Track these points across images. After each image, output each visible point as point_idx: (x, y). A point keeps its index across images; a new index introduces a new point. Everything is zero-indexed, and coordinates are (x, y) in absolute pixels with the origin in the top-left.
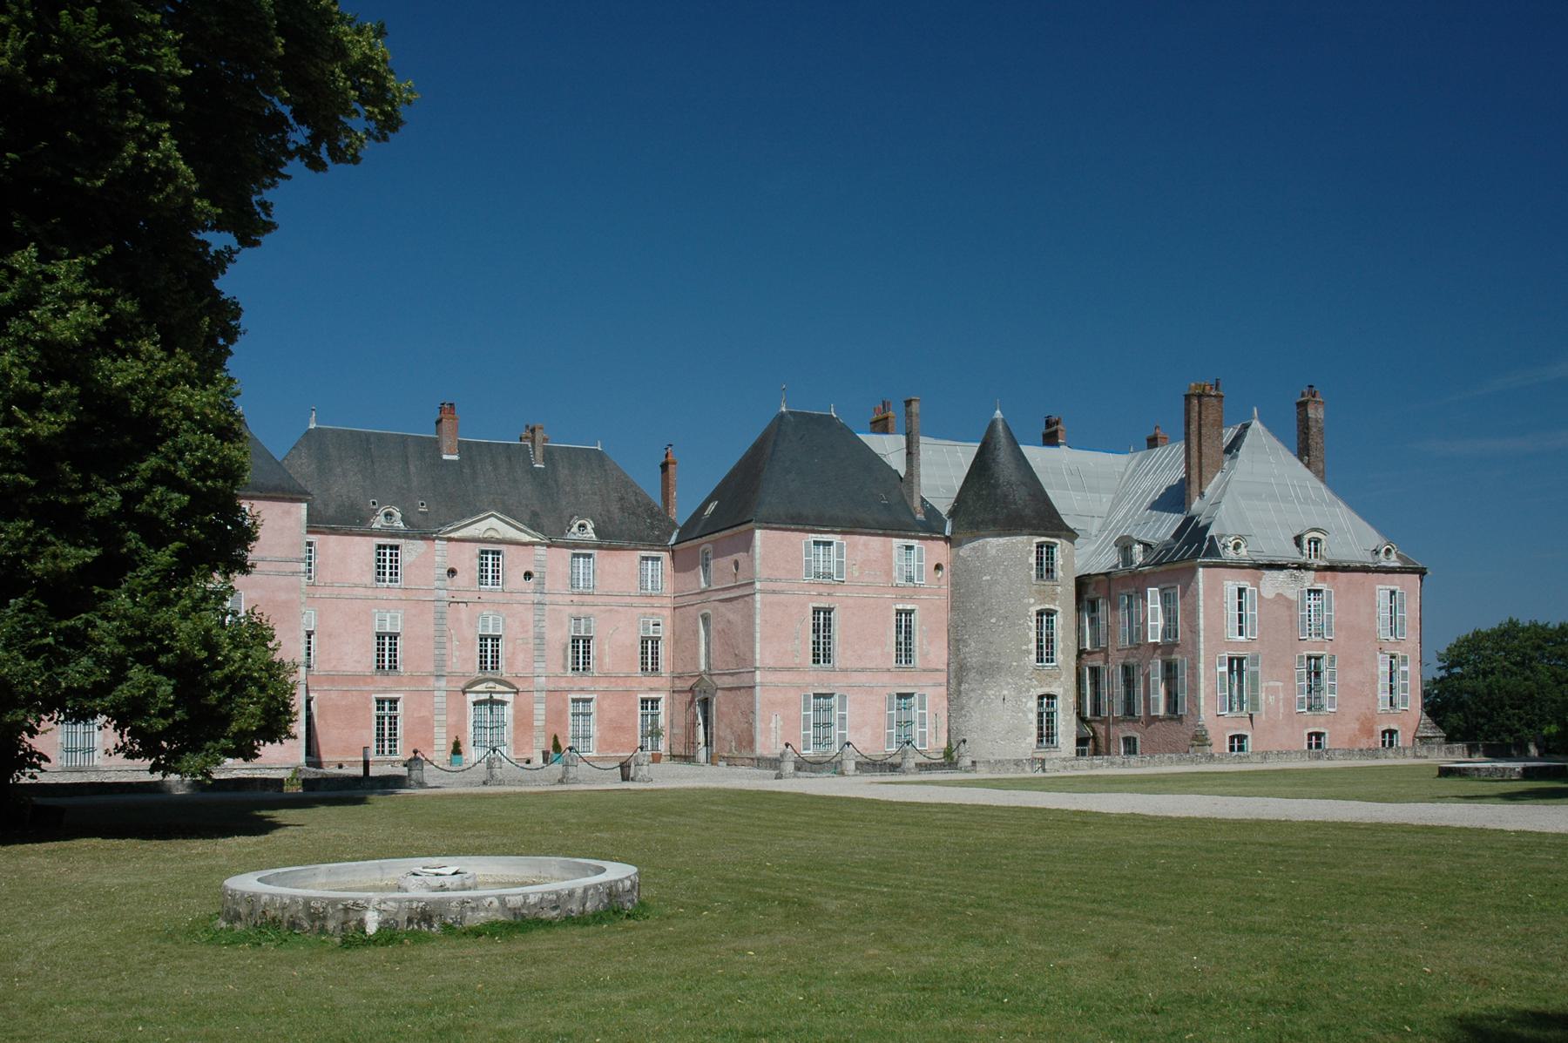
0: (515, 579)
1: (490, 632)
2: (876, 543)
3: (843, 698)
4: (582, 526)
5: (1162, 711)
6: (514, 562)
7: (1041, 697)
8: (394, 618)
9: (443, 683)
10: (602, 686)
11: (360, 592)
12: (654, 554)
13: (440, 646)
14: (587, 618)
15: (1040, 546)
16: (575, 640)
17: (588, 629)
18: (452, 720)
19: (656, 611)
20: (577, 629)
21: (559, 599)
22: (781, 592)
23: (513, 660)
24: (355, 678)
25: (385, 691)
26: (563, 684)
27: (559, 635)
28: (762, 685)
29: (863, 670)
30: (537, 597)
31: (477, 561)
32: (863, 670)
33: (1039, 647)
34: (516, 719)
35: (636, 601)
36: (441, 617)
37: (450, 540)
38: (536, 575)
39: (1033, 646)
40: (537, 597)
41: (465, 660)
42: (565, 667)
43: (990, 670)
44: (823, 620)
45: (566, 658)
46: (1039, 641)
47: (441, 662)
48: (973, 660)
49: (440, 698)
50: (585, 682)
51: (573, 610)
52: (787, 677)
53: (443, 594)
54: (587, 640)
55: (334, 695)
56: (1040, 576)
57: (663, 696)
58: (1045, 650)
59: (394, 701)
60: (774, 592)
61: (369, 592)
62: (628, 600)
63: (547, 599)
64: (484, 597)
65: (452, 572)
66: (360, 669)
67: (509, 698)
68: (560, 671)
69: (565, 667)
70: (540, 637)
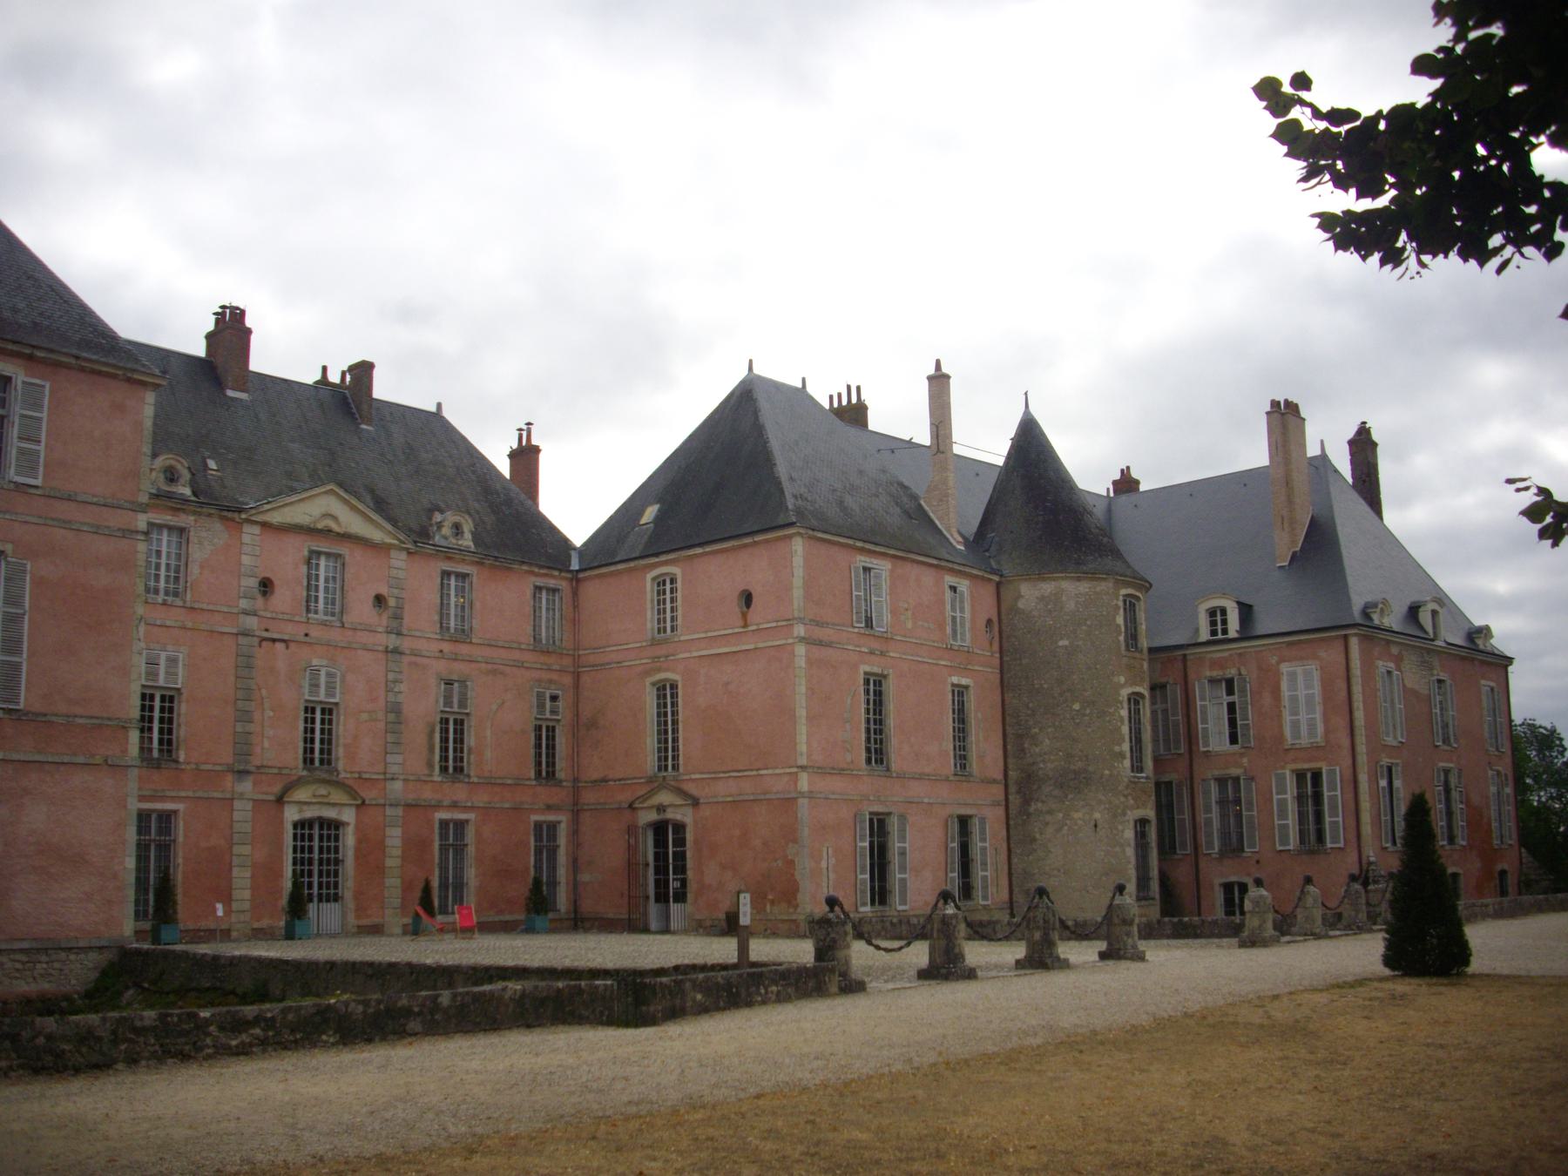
0: (361, 609)
1: (322, 697)
3: (903, 818)
4: (457, 527)
5: (1293, 842)
8: (172, 661)
9: (246, 786)
10: (481, 799)
12: (552, 583)
13: (245, 717)
14: (463, 683)
17: (463, 704)
19: (554, 676)
20: (448, 702)
21: (421, 645)
22: (829, 645)
23: (357, 742)
26: (427, 794)
27: (423, 706)
28: (811, 795)
29: (920, 777)
30: (393, 641)
31: (304, 569)
32: (920, 777)
35: (529, 658)
36: (245, 664)
37: (265, 525)
38: (392, 602)
40: (393, 641)
41: (279, 743)
43: (1075, 781)
45: (431, 749)
47: (243, 747)
50: (460, 792)
51: (440, 666)
53: (251, 623)
54: (459, 723)
57: (563, 819)
59: (166, 818)
60: (820, 643)
62: (517, 655)
63: (406, 644)
64: (316, 633)
65: (266, 586)
67: (348, 816)
69: (430, 765)
70: (395, 709)
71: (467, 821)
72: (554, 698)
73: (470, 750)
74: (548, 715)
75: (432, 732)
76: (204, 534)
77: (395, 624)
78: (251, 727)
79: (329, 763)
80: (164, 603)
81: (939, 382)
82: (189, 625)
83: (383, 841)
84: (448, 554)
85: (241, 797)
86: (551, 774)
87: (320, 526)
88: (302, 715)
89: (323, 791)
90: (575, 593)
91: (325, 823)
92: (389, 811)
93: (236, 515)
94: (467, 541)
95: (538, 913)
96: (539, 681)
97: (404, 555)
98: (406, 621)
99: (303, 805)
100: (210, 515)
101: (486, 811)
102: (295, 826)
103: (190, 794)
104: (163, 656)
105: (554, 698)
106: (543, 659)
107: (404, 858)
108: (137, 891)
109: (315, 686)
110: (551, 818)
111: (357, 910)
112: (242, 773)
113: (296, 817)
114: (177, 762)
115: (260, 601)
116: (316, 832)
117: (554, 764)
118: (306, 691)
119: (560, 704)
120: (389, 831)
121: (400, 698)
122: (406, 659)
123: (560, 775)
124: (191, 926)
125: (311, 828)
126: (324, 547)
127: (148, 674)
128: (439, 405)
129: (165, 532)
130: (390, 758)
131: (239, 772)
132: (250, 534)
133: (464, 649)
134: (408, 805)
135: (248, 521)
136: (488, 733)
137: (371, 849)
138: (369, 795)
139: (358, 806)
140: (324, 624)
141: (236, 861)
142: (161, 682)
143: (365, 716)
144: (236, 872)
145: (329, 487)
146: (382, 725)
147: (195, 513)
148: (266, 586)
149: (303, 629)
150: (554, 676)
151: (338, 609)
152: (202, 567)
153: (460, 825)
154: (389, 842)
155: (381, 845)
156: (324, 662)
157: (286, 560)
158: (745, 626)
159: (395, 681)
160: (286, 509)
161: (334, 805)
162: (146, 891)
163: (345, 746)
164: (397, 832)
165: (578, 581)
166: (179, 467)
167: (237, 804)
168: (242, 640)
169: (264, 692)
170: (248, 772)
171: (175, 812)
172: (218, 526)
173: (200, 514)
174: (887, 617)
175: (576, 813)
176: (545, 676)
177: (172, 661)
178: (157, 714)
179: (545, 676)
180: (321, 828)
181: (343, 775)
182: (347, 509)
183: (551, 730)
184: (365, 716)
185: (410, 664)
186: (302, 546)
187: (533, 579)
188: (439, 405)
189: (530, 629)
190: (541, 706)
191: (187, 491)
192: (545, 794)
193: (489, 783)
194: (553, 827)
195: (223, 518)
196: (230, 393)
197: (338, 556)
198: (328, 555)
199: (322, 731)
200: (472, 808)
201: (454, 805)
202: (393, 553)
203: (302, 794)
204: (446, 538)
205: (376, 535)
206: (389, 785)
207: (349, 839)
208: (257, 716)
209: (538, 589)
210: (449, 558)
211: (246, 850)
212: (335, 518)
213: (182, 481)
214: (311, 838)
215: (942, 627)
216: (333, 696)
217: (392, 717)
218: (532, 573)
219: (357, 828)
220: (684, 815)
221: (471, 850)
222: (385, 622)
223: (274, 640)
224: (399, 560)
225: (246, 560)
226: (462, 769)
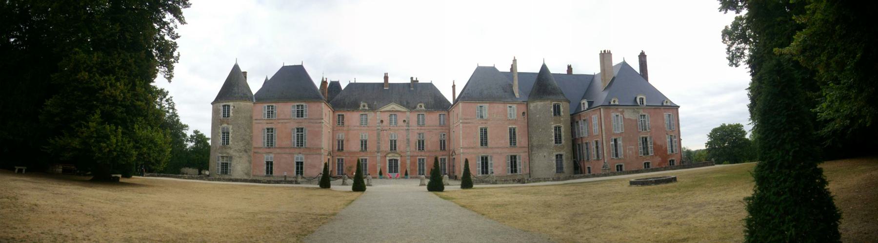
0: (400, 123)
2: (501, 106)
6: (401, 118)
7: (557, 156)
10: (427, 154)
15: (554, 106)
23: (400, 146)
24: (354, 153)
27: (414, 138)
33: (556, 139)
36: (378, 135)
39: (554, 138)
41: (386, 146)
43: (540, 147)
44: (484, 133)
46: (556, 136)
47: (379, 148)
48: (535, 144)
49: (379, 158)
50: (423, 153)
52: (471, 150)
56: (555, 115)
57: (447, 158)
58: (558, 139)
65: (382, 121)
67: (399, 158)
70: (408, 140)
81: (515, 61)
84: (418, 111)
94: (423, 108)
99: (391, 156)
132: (378, 113)
148: (382, 121)
151: (396, 123)
174: (487, 115)
186: (389, 114)
193: (429, 151)
207: (399, 162)
215: (506, 116)
224: (408, 113)
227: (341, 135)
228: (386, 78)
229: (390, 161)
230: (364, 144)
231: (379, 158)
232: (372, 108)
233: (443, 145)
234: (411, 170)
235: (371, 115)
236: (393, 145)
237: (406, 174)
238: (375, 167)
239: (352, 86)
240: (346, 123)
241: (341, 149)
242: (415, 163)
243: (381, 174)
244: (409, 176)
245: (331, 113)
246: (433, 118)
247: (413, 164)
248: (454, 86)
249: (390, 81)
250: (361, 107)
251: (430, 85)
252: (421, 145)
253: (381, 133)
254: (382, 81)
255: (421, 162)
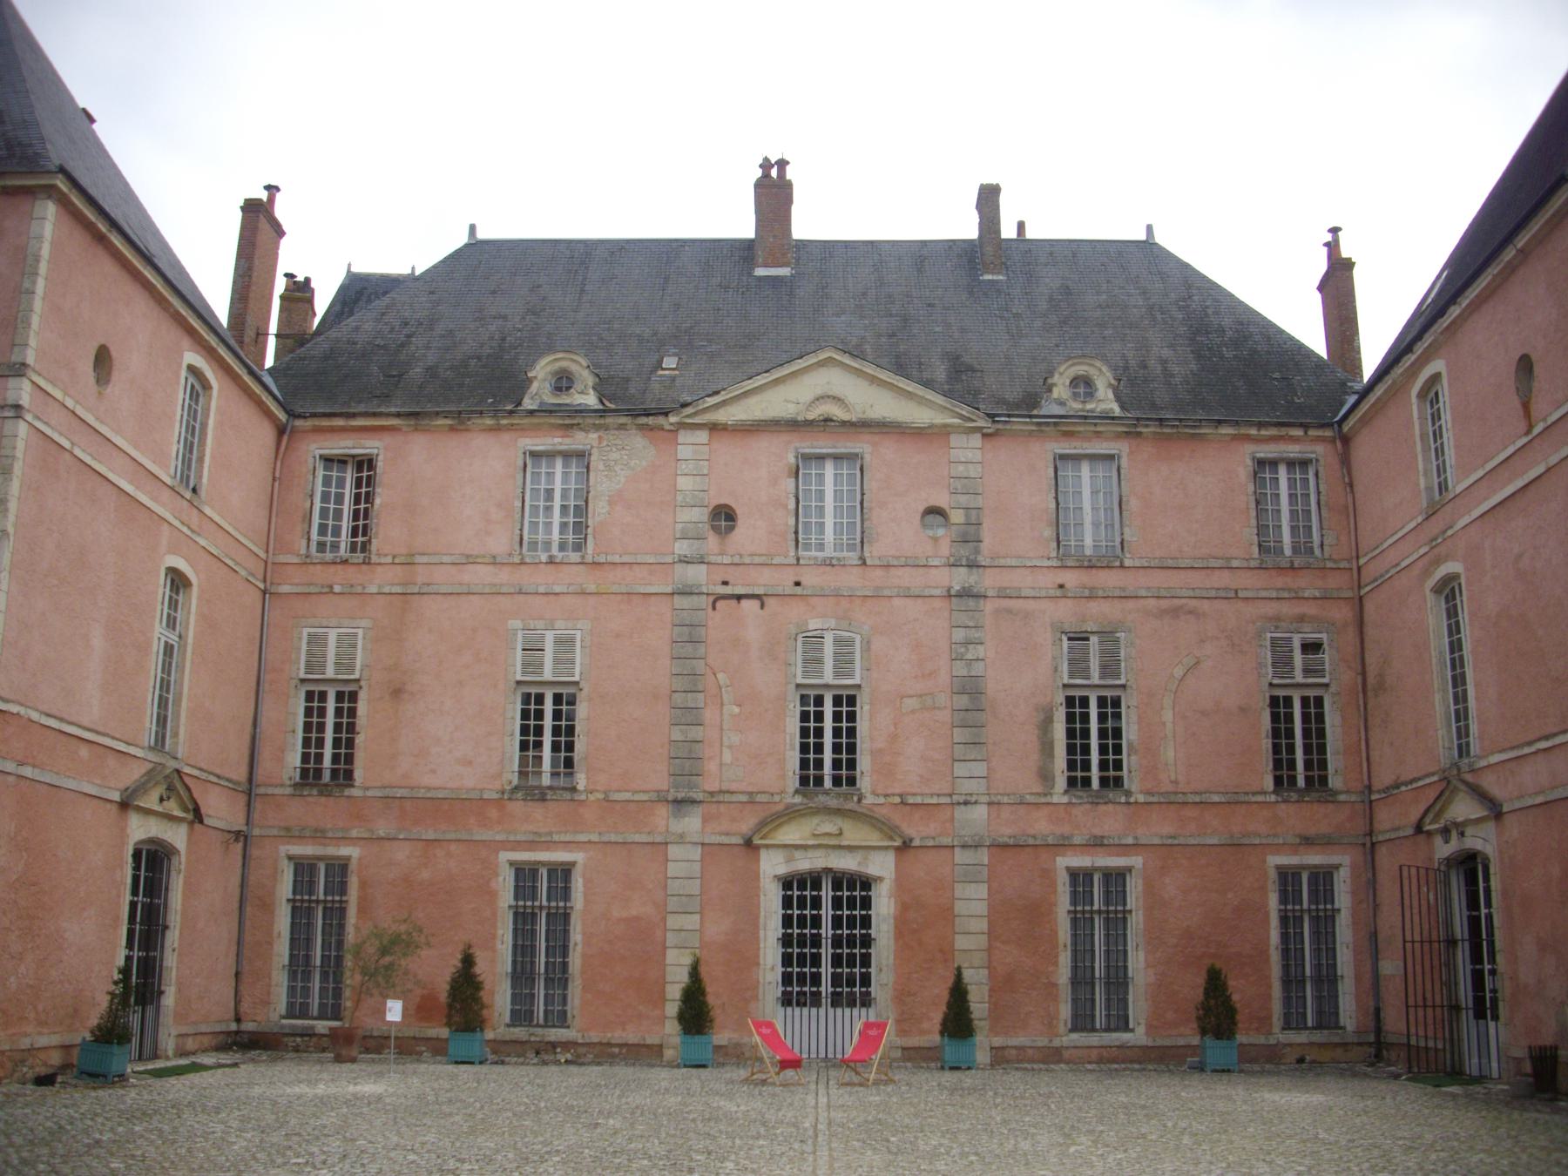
0: (898, 530)
1: (828, 677)
4: (1083, 385)
8: (564, 643)
9: (691, 823)
10: (1158, 829)
11: (481, 575)
12: (1293, 450)
13: (689, 716)
14: (1108, 635)
16: (1076, 707)
18: (718, 928)
19: (1310, 609)
20: (1078, 665)
21: (1023, 581)
25: (531, 845)
26: (1041, 826)
30: (960, 578)
34: (902, 927)
35: (1249, 582)
36: (690, 637)
37: (714, 428)
38: (957, 517)
40: (960, 578)
41: (755, 750)
42: (1046, 776)
45: (1047, 748)
47: (687, 763)
49: (683, 863)
50: (1109, 820)
51: (1064, 612)
53: (696, 574)
54: (1111, 707)
55: (402, 853)
57: (1345, 864)
59: (562, 875)
61: (503, 576)
62: (1223, 579)
63: (988, 581)
64: (811, 578)
65: (724, 517)
66: (468, 780)
67: (881, 866)
68: (1028, 784)
69: (1046, 776)
70: (971, 690)
71: (1130, 869)
72: (1311, 647)
73: (1130, 745)
74: (1299, 679)
75: (1048, 721)
76: (615, 455)
77: (965, 551)
78: (696, 733)
79: (852, 781)
80: (551, 561)
82: (592, 588)
83: (952, 908)
84: (1063, 426)
85: (681, 839)
86: (1318, 781)
87: (810, 417)
88: (795, 710)
89: (829, 826)
90: (1346, 461)
91: (841, 880)
92: (960, 856)
93: (661, 420)
94: (1106, 400)
95: (1219, 1035)
96: (1277, 619)
97: (976, 440)
98: (987, 545)
100: (622, 427)
101: (1167, 850)
102: (787, 884)
103: (594, 838)
104: (549, 637)
105: (1311, 647)
106: (1280, 581)
107: (991, 934)
108: (293, 975)
109: (813, 661)
110: (1315, 859)
111: (898, 1022)
112: (681, 804)
113: (782, 870)
114: (574, 789)
115: (712, 541)
116: (827, 893)
117: (1323, 764)
118: (799, 673)
119: (1327, 656)
120: (959, 890)
121: (978, 669)
122: (989, 606)
123: (1334, 782)
124: (594, 1036)
125: (817, 885)
126: (822, 445)
127: (525, 665)
128: (1149, 228)
129: (559, 463)
130: (960, 770)
131: (676, 802)
132: (691, 445)
133: (1109, 580)
134: (999, 847)
135: (682, 426)
136: (1168, 716)
137: (927, 920)
138: (916, 830)
139: (897, 849)
140: (829, 563)
141: (671, 939)
142: (548, 675)
143: (911, 703)
144: (671, 956)
145: (823, 356)
146: (945, 716)
147: (597, 428)
149: (789, 576)
150: (1310, 609)
152: (610, 503)
153: (1115, 880)
154: (960, 907)
155: (947, 914)
156: (832, 623)
157: (758, 477)
158: (1530, 427)
159: (967, 643)
160: (752, 400)
161: (851, 848)
162: (307, 976)
163: (877, 753)
164: (982, 891)
165: (1346, 440)
166: (574, 368)
167: (674, 851)
168: (679, 601)
169: (720, 676)
170: (693, 802)
171: (573, 864)
172: (638, 441)
173: (606, 428)
175: (1370, 847)
176: (1287, 609)
177: (564, 643)
178: (548, 722)
179: (1287, 609)
180: (837, 885)
181: (869, 800)
182: (863, 384)
183: (1313, 707)
184: (911, 703)
185: (997, 611)
186: (786, 450)
187: (1249, 448)
188: (1149, 228)
189: (1250, 534)
190: (1282, 662)
191: (591, 400)
192: (1298, 816)
193: (1173, 802)
194: (1322, 880)
195: (641, 427)
196: (760, 272)
197: (851, 457)
198: (837, 458)
199: (837, 732)
200: (1136, 847)
201: (1097, 843)
202: (955, 440)
203: (791, 834)
204: (1062, 403)
205: (921, 415)
206: (960, 812)
207: (883, 906)
208: (709, 715)
209: (1261, 463)
210: (1069, 435)
211: (693, 921)
212: (837, 399)
213: (578, 386)
214: (817, 903)
216: (851, 675)
217: (963, 701)
218: (1248, 438)
219: (902, 884)
220: (1482, 840)
221: (1136, 922)
222: (945, 549)
223: (739, 598)
224: (967, 450)
225: (684, 483)
226: (1118, 782)
227: (341, 637)
228: (774, 192)
229: (799, 888)
230: (548, 722)
231: (683, 863)
232: (635, 406)
233: (1296, 744)
234: (1003, 984)
235: (622, 461)
236: (829, 744)
237: (958, 1023)
238: (645, 940)
239: (479, 261)
240: (388, 534)
241: (329, 767)
242: (1036, 912)
243: (695, 1015)
244: (983, 1043)
245: (264, 434)
246: (1200, 494)
247: (1017, 919)
248: (1337, 284)
249: (807, 224)
250: (539, 391)
251: (1143, 260)
252: (1092, 742)
253: (717, 622)
254: (741, 224)
255: (1097, 897)
